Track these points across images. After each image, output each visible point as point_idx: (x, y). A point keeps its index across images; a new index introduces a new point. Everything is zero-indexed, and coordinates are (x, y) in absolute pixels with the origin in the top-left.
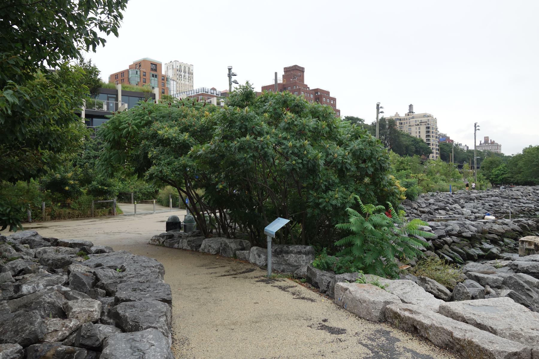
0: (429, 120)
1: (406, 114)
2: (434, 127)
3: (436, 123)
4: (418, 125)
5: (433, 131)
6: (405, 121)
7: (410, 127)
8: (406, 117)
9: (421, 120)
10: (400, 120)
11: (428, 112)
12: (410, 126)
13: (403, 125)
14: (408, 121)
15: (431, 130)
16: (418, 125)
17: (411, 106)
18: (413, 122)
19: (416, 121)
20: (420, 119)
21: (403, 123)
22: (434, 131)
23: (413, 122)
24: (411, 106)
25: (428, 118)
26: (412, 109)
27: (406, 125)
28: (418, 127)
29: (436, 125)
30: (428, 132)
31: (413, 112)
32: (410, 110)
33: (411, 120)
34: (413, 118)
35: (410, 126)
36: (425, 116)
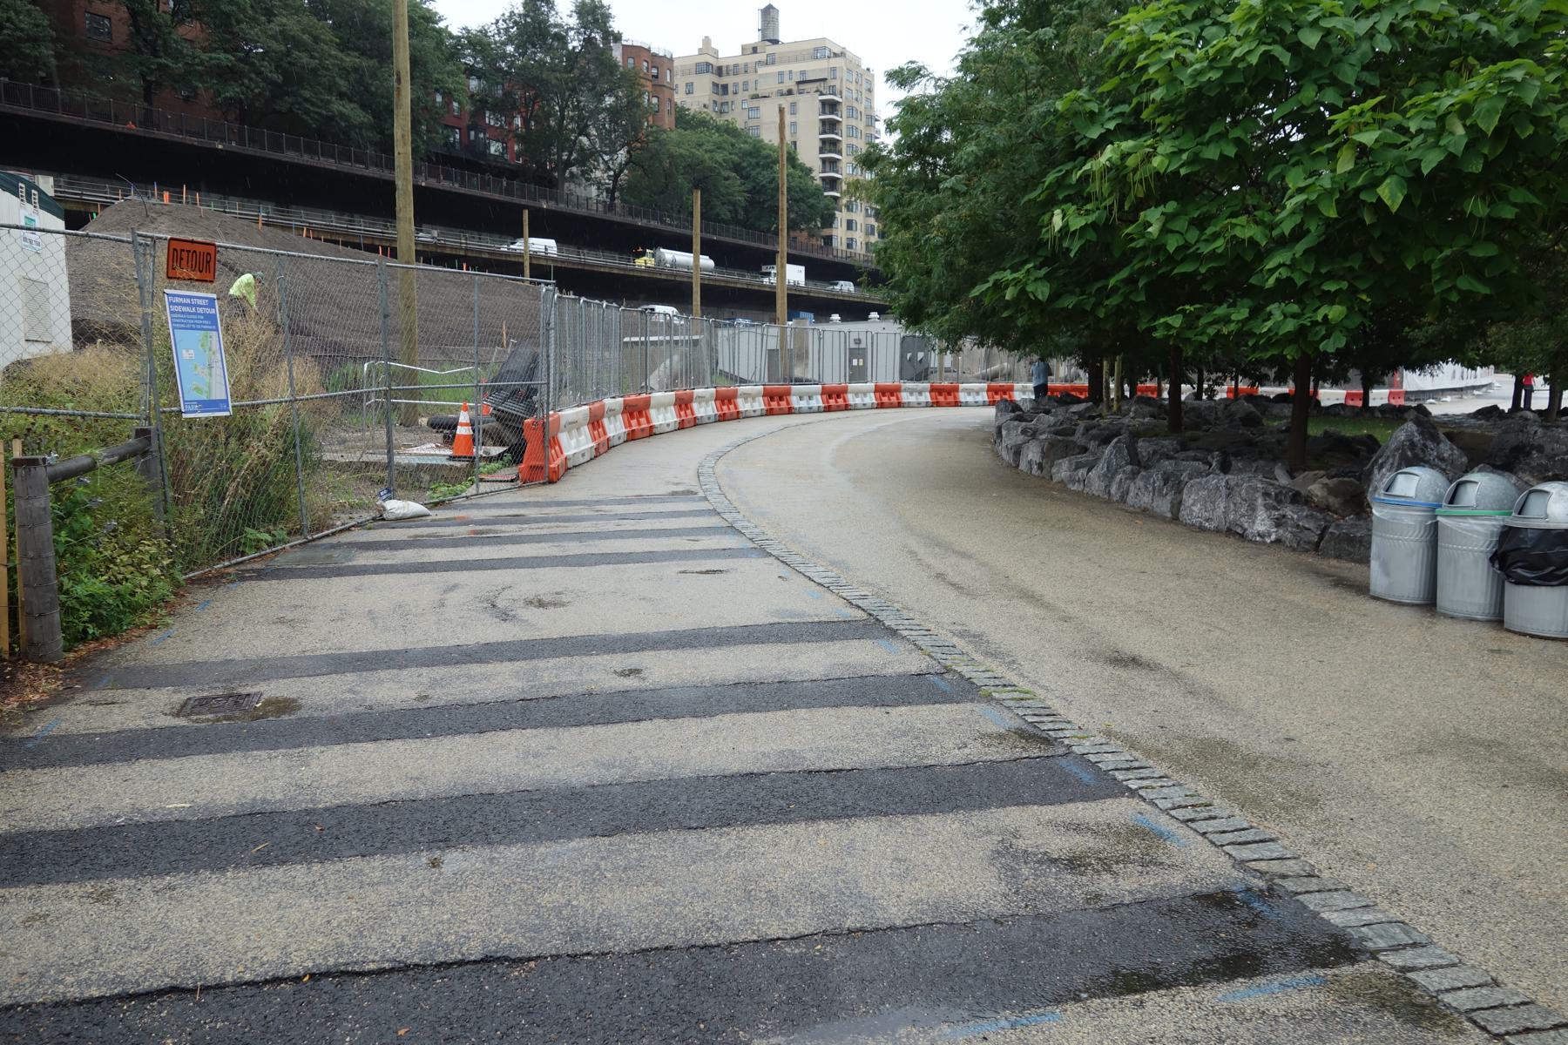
0: (834, 70)
1: (744, 48)
2: (861, 108)
3: (870, 91)
4: (790, 92)
5: (853, 122)
6: (740, 79)
7: (755, 103)
8: (741, 61)
9: (803, 73)
10: (719, 71)
11: (839, 38)
12: (755, 97)
13: (728, 98)
14: (750, 77)
15: (842, 117)
16: (790, 92)
17: (769, 13)
18: (767, 77)
19: (781, 74)
20: (797, 67)
21: (731, 89)
22: (861, 125)
23: (767, 77)
24: (769, 13)
25: (835, 62)
26: (776, 29)
27: (742, 95)
28: (785, 102)
29: (869, 100)
30: (830, 126)
31: (775, 42)
32: (763, 30)
33: (761, 70)
34: (771, 61)
35: (755, 97)
36: (819, 50)
